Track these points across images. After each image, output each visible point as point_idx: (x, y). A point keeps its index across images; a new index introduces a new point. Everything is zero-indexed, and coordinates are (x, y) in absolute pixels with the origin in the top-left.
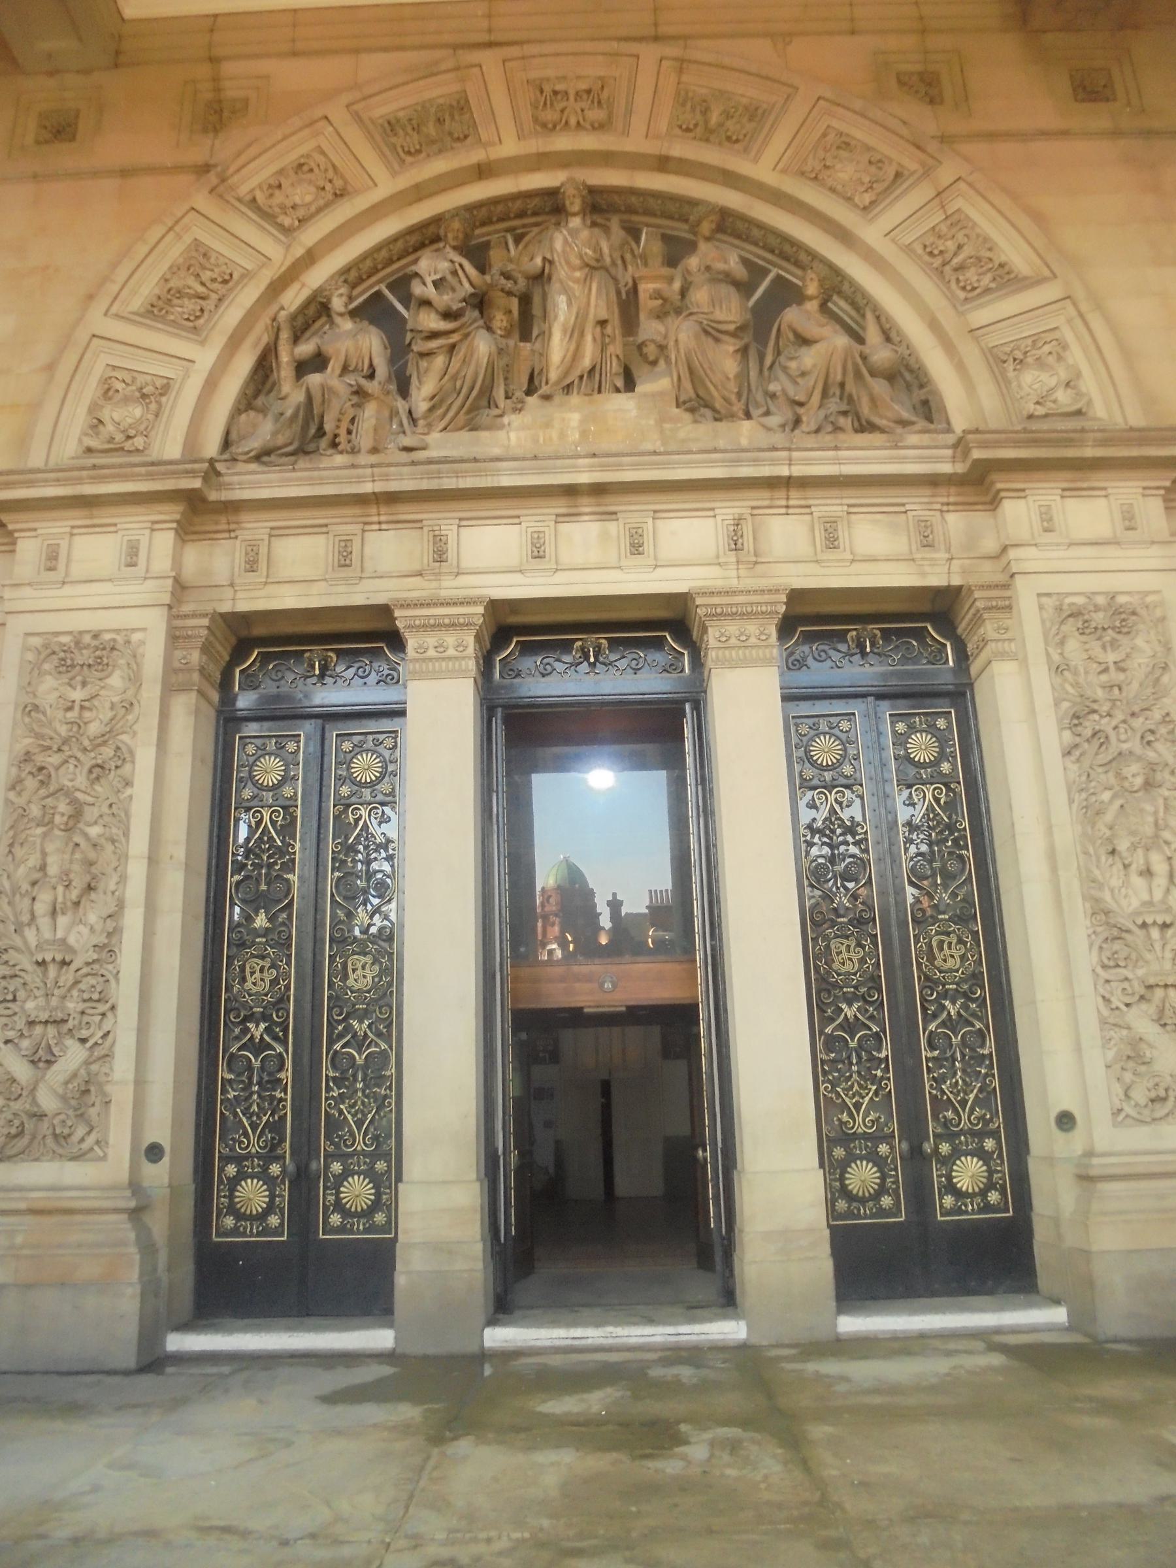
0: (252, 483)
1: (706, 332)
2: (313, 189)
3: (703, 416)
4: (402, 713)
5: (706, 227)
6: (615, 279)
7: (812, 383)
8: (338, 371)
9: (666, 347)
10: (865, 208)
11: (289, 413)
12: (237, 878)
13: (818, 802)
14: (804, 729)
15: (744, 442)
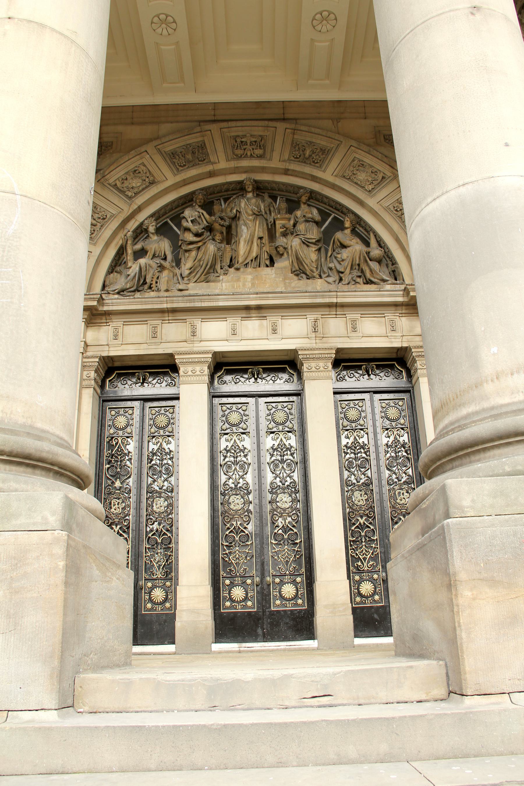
0: (114, 303)
1: (304, 243)
2: (141, 181)
3: (302, 277)
4: (178, 398)
5: (304, 199)
6: (266, 220)
7: (346, 264)
8: (151, 257)
9: (287, 248)
10: (370, 191)
11: (132, 275)
12: (108, 466)
13: (349, 436)
14: (343, 406)
15: (319, 289)
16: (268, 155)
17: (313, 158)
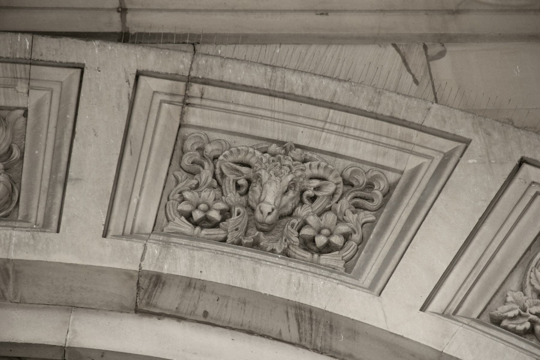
16: (35, 205)
17: (305, 224)
